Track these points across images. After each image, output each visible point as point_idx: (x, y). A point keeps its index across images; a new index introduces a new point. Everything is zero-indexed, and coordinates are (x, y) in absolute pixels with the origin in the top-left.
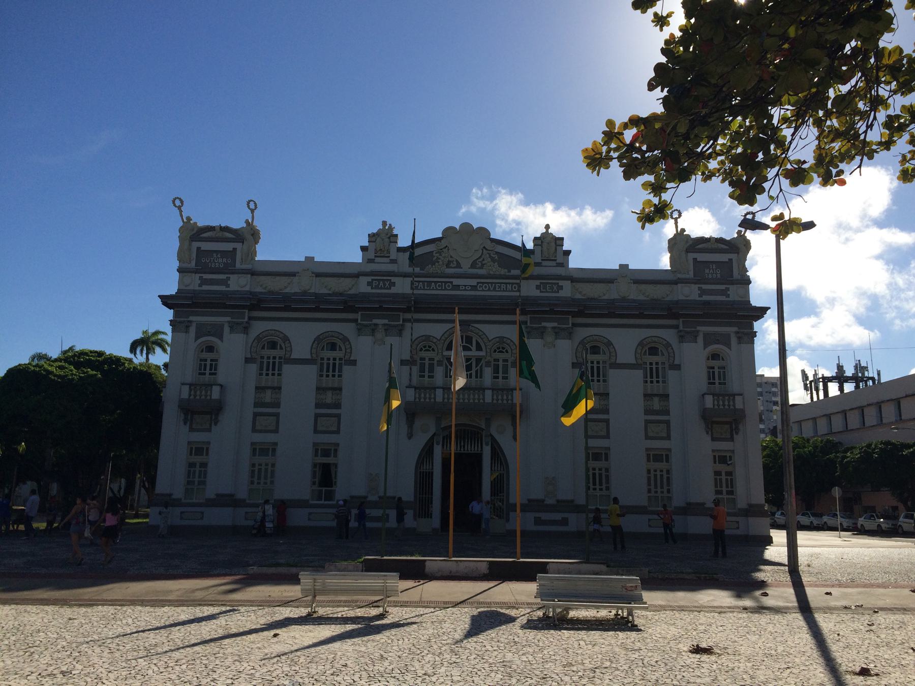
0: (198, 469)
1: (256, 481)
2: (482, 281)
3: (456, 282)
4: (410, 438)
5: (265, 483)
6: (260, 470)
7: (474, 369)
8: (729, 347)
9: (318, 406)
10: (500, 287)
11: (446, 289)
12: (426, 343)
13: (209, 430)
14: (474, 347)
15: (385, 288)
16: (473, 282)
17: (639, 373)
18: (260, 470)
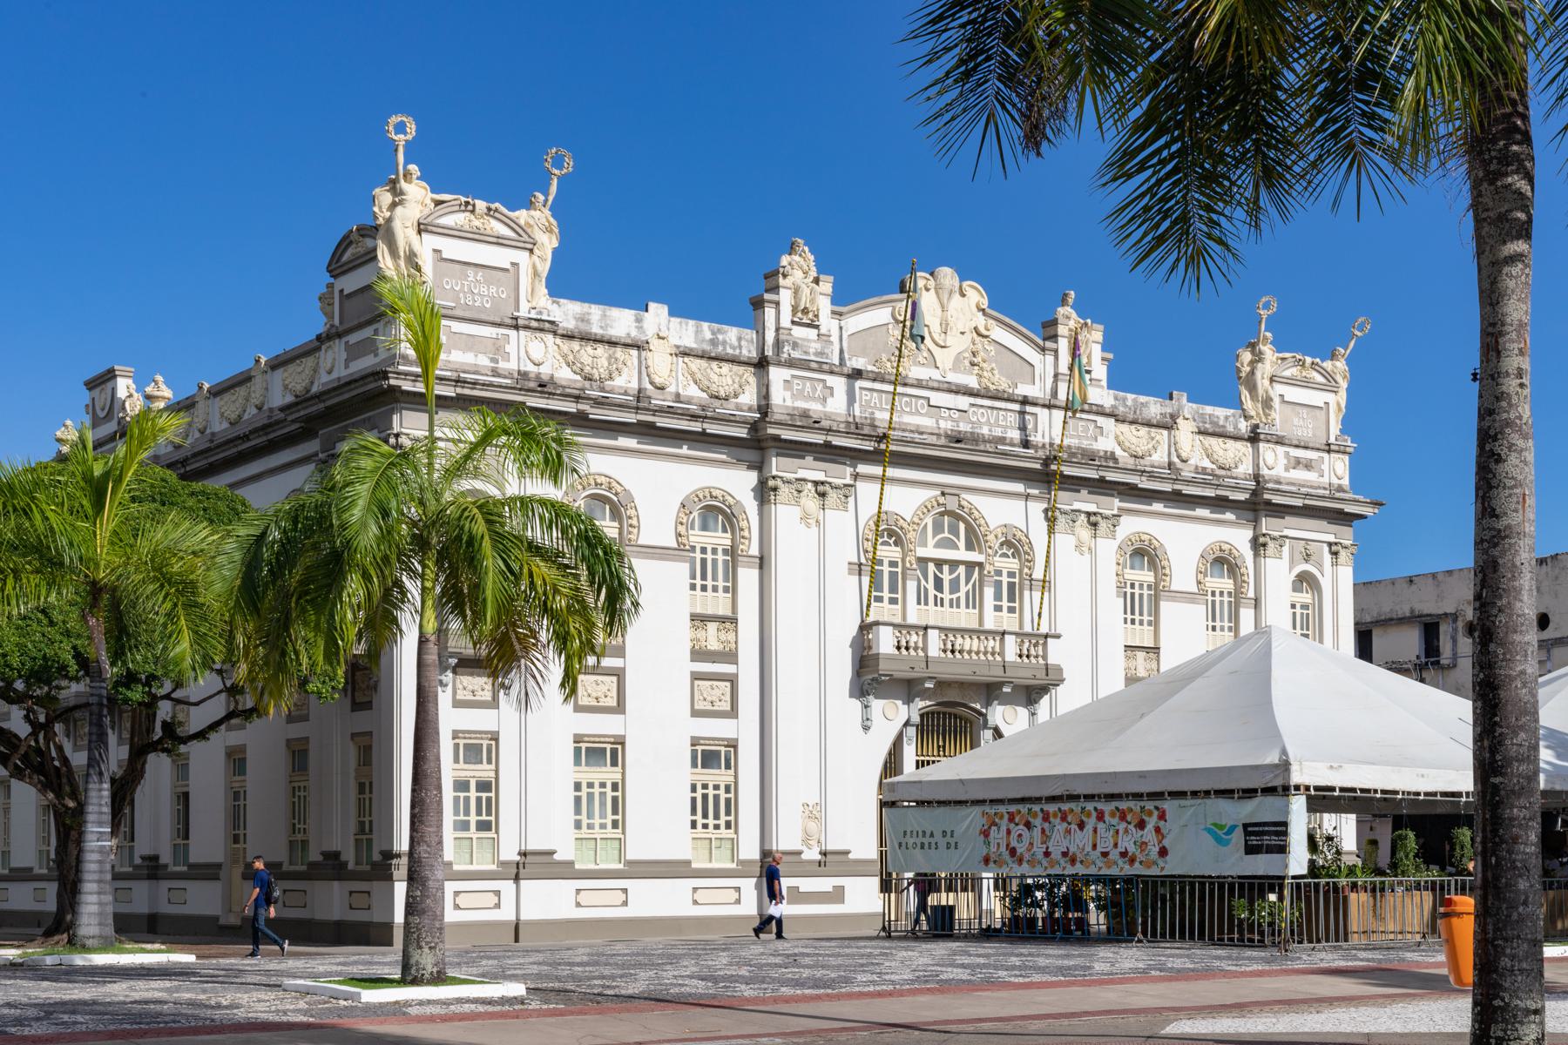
0: (473, 794)
1: (585, 822)
2: (979, 401)
3: (938, 398)
4: (866, 728)
5: (603, 826)
6: (590, 796)
7: (963, 588)
8: (1320, 566)
9: (698, 654)
10: (1005, 418)
11: (918, 413)
12: (887, 530)
13: (494, 704)
14: (962, 543)
15: (813, 399)
16: (963, 402)
17: (1199, 611)
18: (590, 796)
